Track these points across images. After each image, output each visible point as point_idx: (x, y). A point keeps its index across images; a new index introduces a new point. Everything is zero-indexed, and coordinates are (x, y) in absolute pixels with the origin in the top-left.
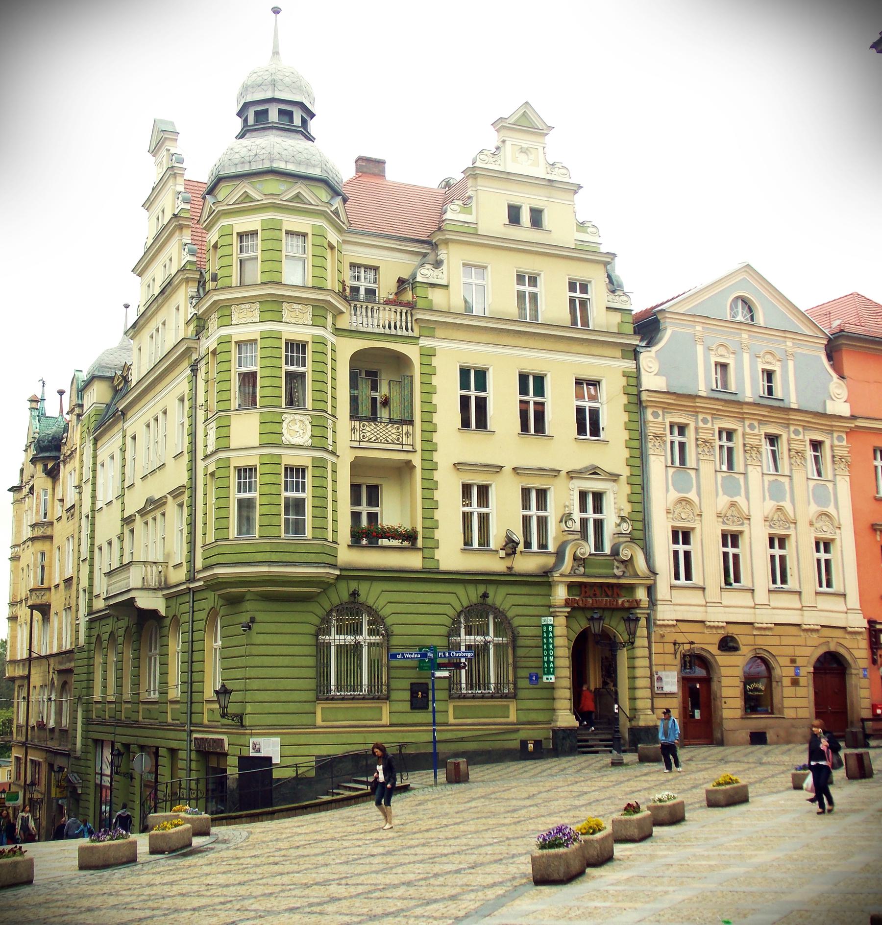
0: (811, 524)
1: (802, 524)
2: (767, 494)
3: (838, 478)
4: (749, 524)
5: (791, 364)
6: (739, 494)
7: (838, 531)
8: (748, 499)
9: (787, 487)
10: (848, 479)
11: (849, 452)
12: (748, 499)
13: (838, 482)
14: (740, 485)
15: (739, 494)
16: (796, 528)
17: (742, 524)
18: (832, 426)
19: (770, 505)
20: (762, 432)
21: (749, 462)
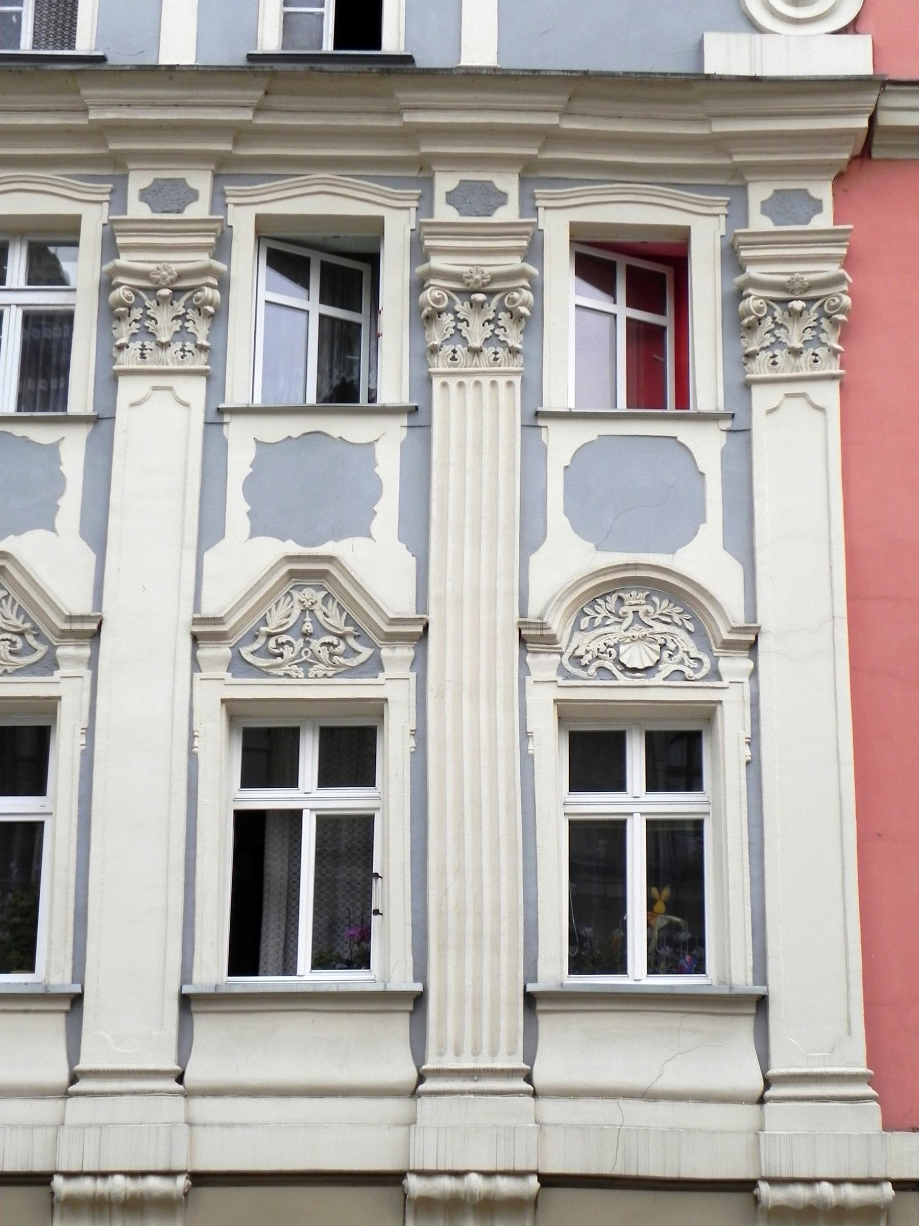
0: (531, 638)
2: (237, 508)
3: (762, 398)
4: (93, 663)
6: (45, 518)
7: (735, 666)
8: (97, 535)
9: (389, 464)
10: (829, 396)
11: (847, 262)
12: (97, 535)
14: (59, 483)
15: (45, 518)
16: (420, 664)
17: (49, 664)
18: (720, 143)
19: (246, 561)
20: (243, 223)
21: (128, 360)
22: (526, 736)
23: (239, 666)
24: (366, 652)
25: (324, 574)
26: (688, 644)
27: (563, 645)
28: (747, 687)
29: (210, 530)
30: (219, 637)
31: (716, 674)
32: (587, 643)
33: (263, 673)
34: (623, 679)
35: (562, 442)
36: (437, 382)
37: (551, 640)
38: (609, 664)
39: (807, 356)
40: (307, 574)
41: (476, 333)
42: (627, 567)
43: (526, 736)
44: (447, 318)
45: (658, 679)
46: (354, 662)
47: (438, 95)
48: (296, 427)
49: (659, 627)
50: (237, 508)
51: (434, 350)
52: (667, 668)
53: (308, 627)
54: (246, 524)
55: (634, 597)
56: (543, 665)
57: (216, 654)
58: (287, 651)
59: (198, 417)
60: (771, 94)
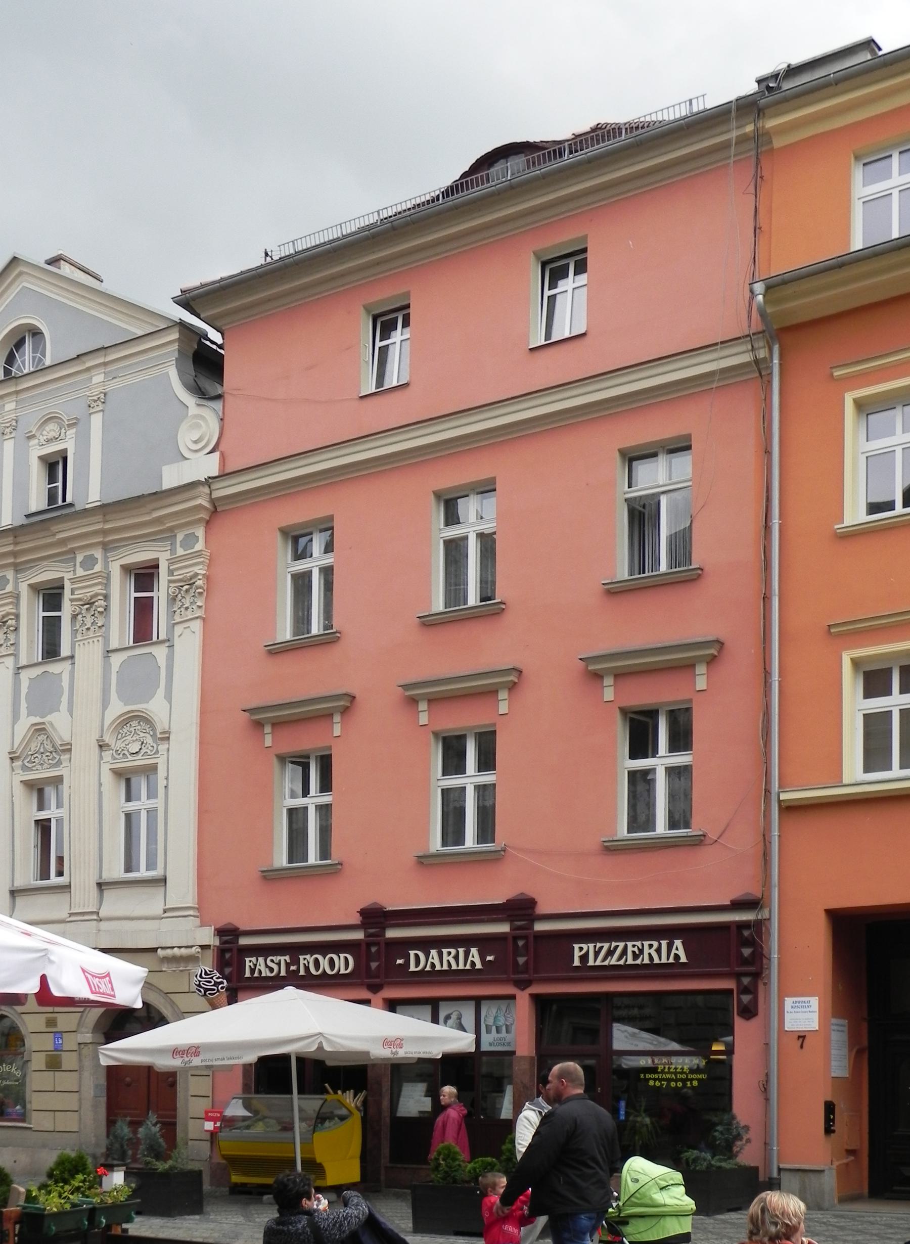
0: (102, 746)
1: (84, 751)
2: (24, 705)
5: (97, 421)
13: (177, 642)
18: (159, 520)
22: (100, 785)
23: (25, 768)
24: (58, 757)
25: (44, 729)
26: (149, 740)
27: (112, 747)
28: (166, 756)
29: (16, 717)
30: (18, 758)
31: (157, 752)
32: (120, 745)
33: (30, 769)
34: (130, 758)
35: (117, 660)
36: (77, 644)
37: (108, 745)
38: (126, 752)
39: (190, 609)
40: (40, 730)
41: (89, 621)
42: (129, 712)
43: (100, 785)
44: (80, 616)
45: (140, 757)
46: (54, 762)
47: (65, 525)
48: (38, 671)
49: (142, 735)
50: (24, 705)
51: (77, 630)
52: (142, 752)
53: (42, 750)
54: (26, 712)
55: (134, 723)
56: (107, 755)
57: (18, 763)
58: (36, 760)
59: (11, 672)
60: (175, 494)
